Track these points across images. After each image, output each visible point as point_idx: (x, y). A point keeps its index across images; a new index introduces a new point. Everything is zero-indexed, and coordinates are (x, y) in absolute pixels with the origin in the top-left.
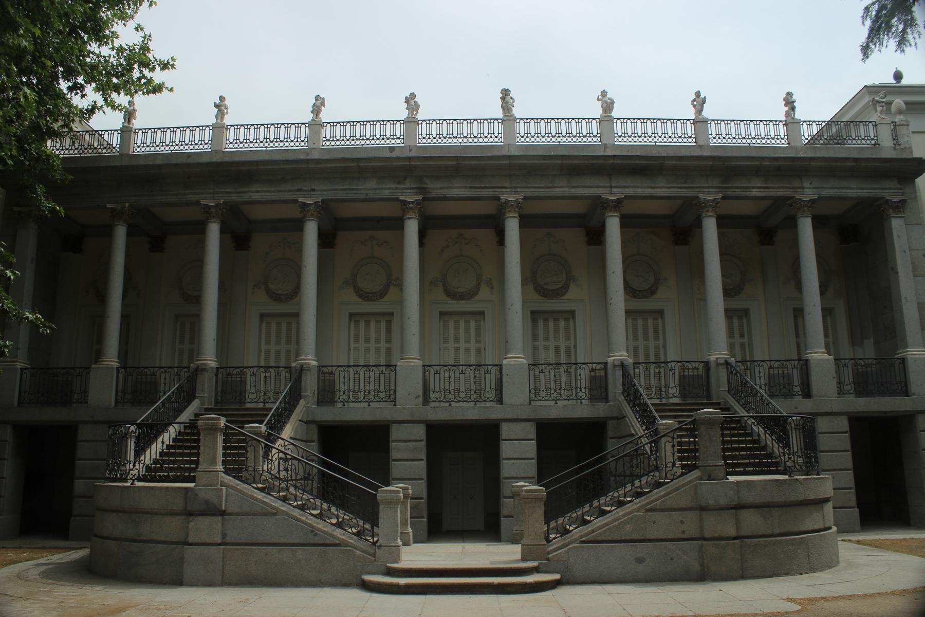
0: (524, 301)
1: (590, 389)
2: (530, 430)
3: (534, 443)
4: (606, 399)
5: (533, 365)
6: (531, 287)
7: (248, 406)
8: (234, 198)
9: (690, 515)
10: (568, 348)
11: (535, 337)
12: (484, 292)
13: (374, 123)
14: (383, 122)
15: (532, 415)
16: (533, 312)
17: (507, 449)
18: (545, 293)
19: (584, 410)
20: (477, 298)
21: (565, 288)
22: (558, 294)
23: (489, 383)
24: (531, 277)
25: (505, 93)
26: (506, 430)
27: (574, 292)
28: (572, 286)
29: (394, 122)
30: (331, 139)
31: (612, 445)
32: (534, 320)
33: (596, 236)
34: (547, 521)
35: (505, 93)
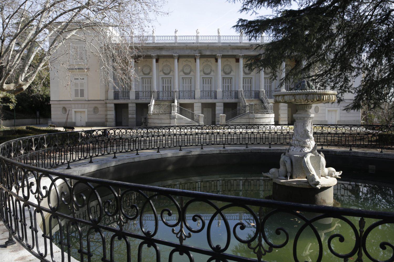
0: (222, 75)
1: (235, 96)
2: (222, 104)
3: (223, 107)
4: (238, 98)
5: (223, 91)
6: (223, 72)
7: (160, 99)
8: (159, 54)
9: (248, 119)
10: (230, 86)
11: (223, 83)
12: (212, 73)
13: (189, 36)
14: (191, 36)
15: (223, 101)
16: (223, 78)
17: (217, 108)
18: (226, 73)
19: (233, 101)
20: (211, 74)
21: (230, 72)
22: (229, 74)
23: (213, 94)
24: (223, 70)
25: (218, 29)
26: (217, 104)
27: (232, 73)
28: (232, 72)
29: (194, 36)
30: (179, 40)
31: (238, 107)
32: (223, 79)
33: (238, 61)
34: (226, 121)
35: (218, 29)
